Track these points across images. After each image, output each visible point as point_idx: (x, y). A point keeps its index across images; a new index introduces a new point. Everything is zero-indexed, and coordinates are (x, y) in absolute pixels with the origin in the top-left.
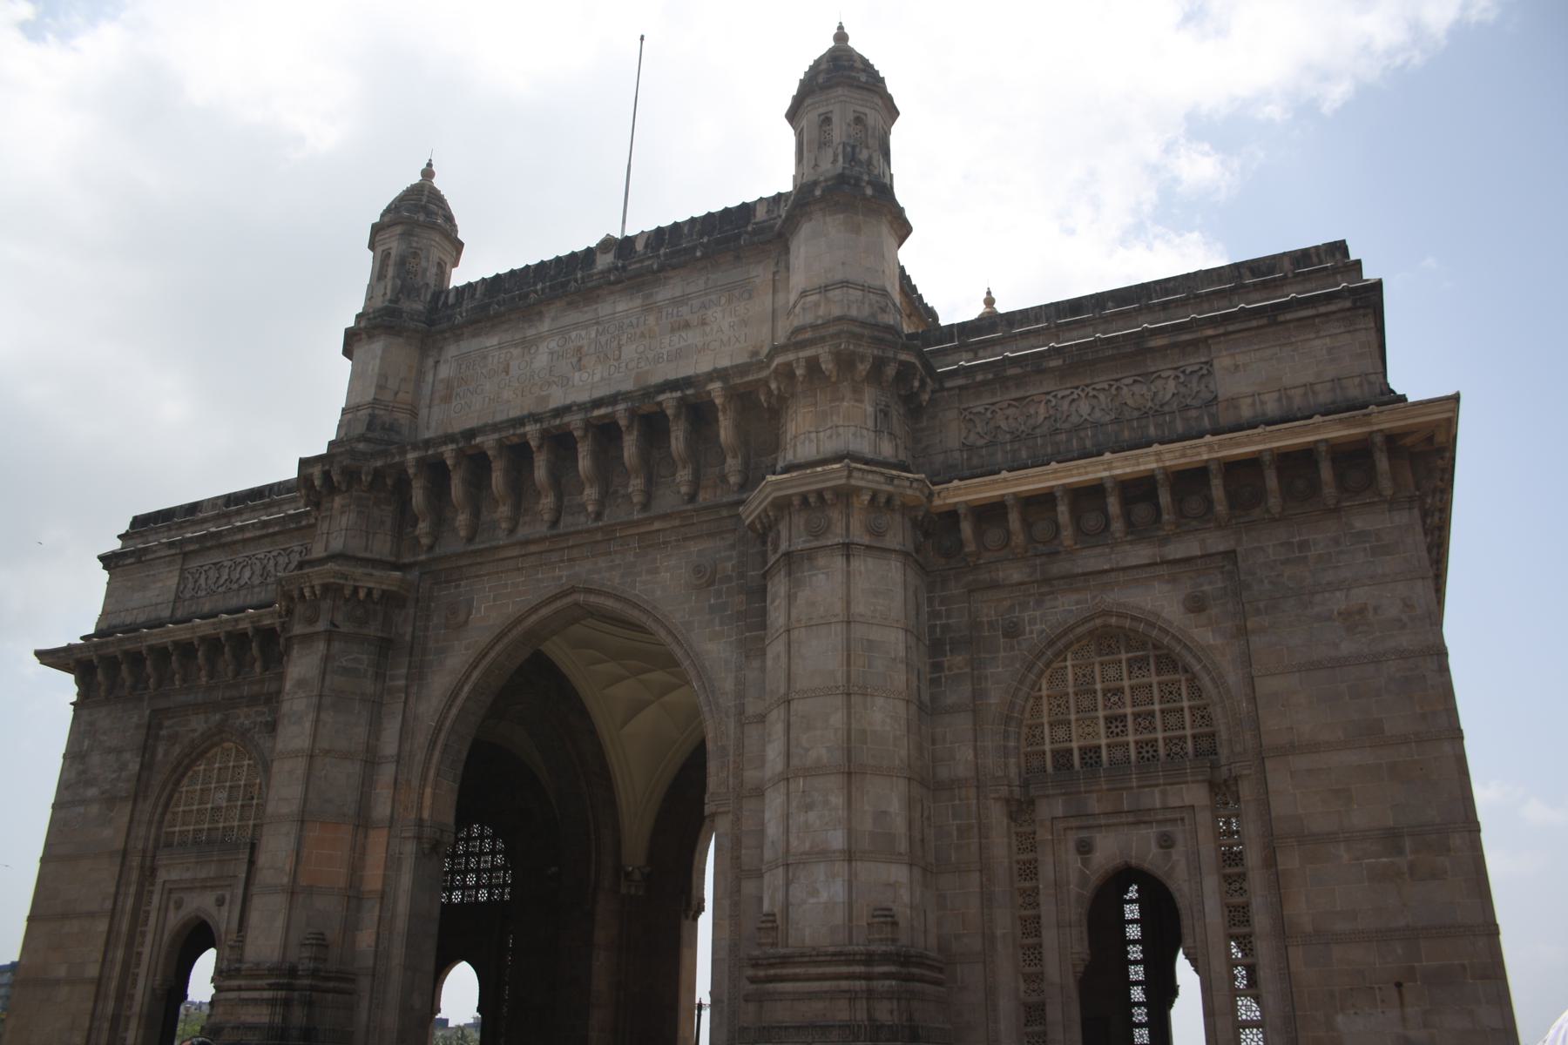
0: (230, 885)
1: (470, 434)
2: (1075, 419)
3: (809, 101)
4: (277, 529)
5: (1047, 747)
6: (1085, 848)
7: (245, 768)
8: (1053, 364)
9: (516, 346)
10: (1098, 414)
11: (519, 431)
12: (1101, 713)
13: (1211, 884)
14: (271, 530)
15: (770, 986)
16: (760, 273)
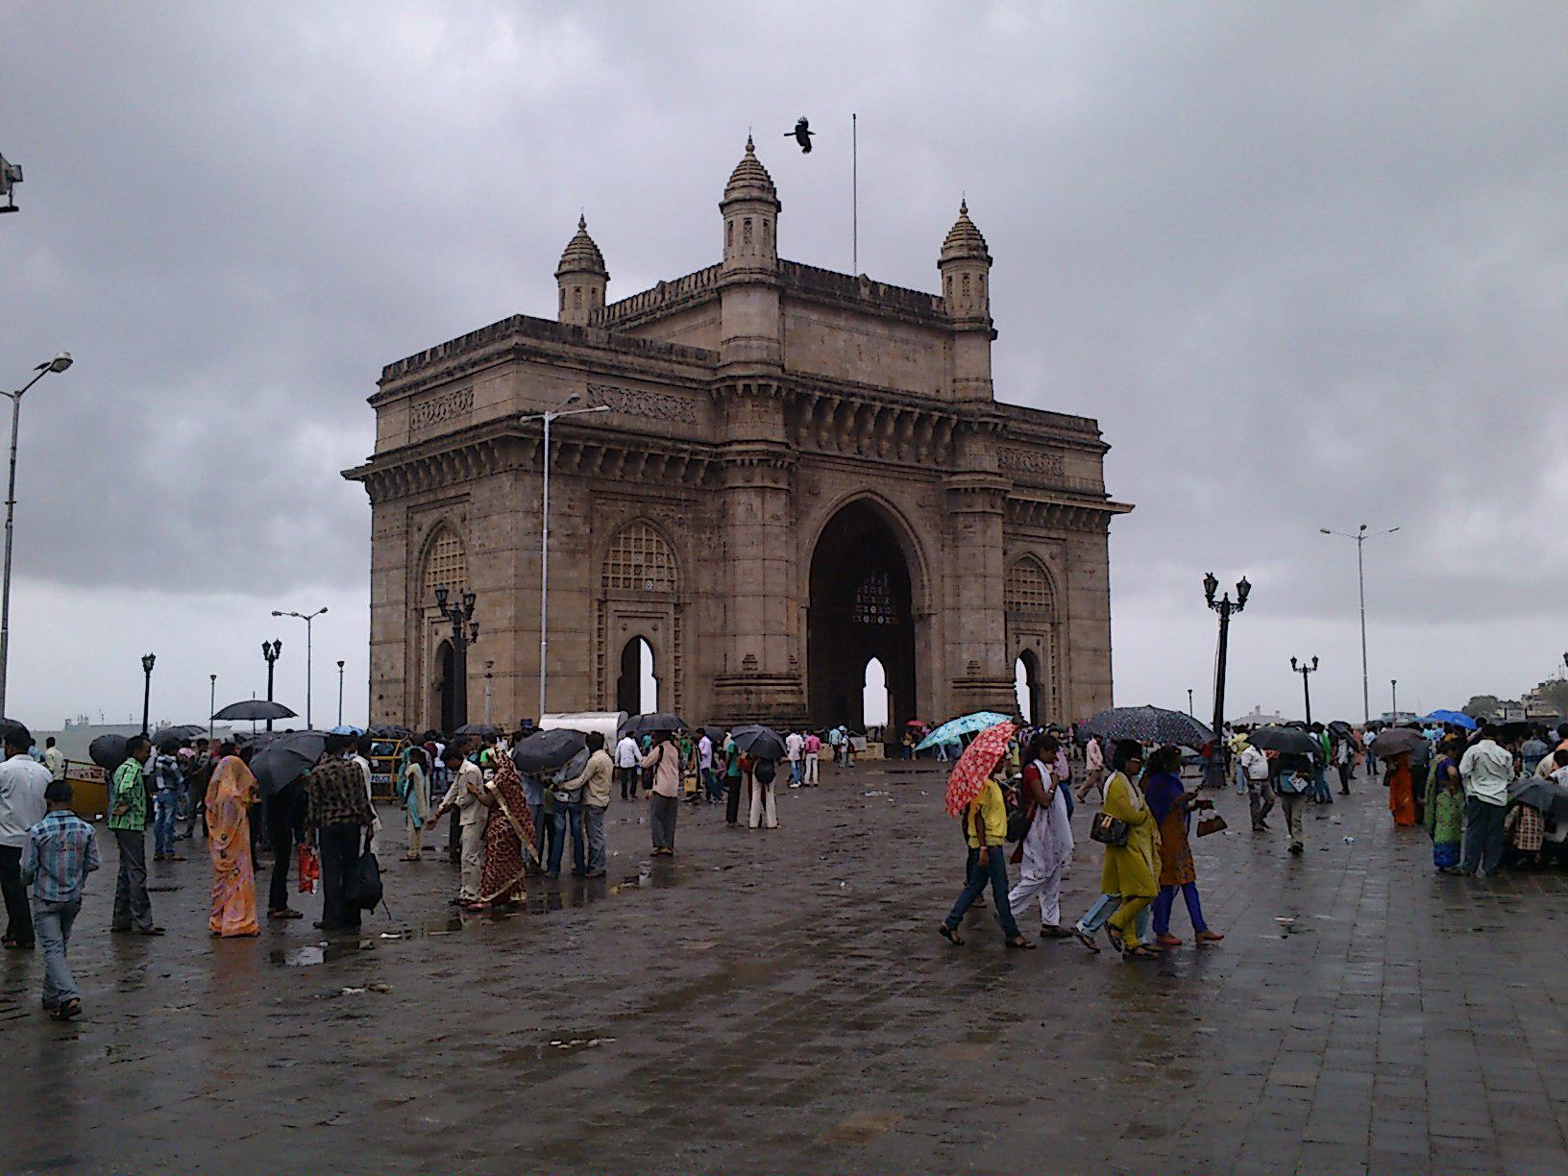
0: (662, 618)
1: (853, 395)
2: (1022, 466)
3: (975, 263)
4: (668, 382)
5: (1007, 601)
6: (1018, 643)
7: (654, 542)
8: (1023, 439)
9: (827, 327)
10: (1029, 467)
11: (873, 403)
12: (1022, 590)
13: (1050, 658)
14: (663, 381)
15: (987, 690)
16: (939, 344)
